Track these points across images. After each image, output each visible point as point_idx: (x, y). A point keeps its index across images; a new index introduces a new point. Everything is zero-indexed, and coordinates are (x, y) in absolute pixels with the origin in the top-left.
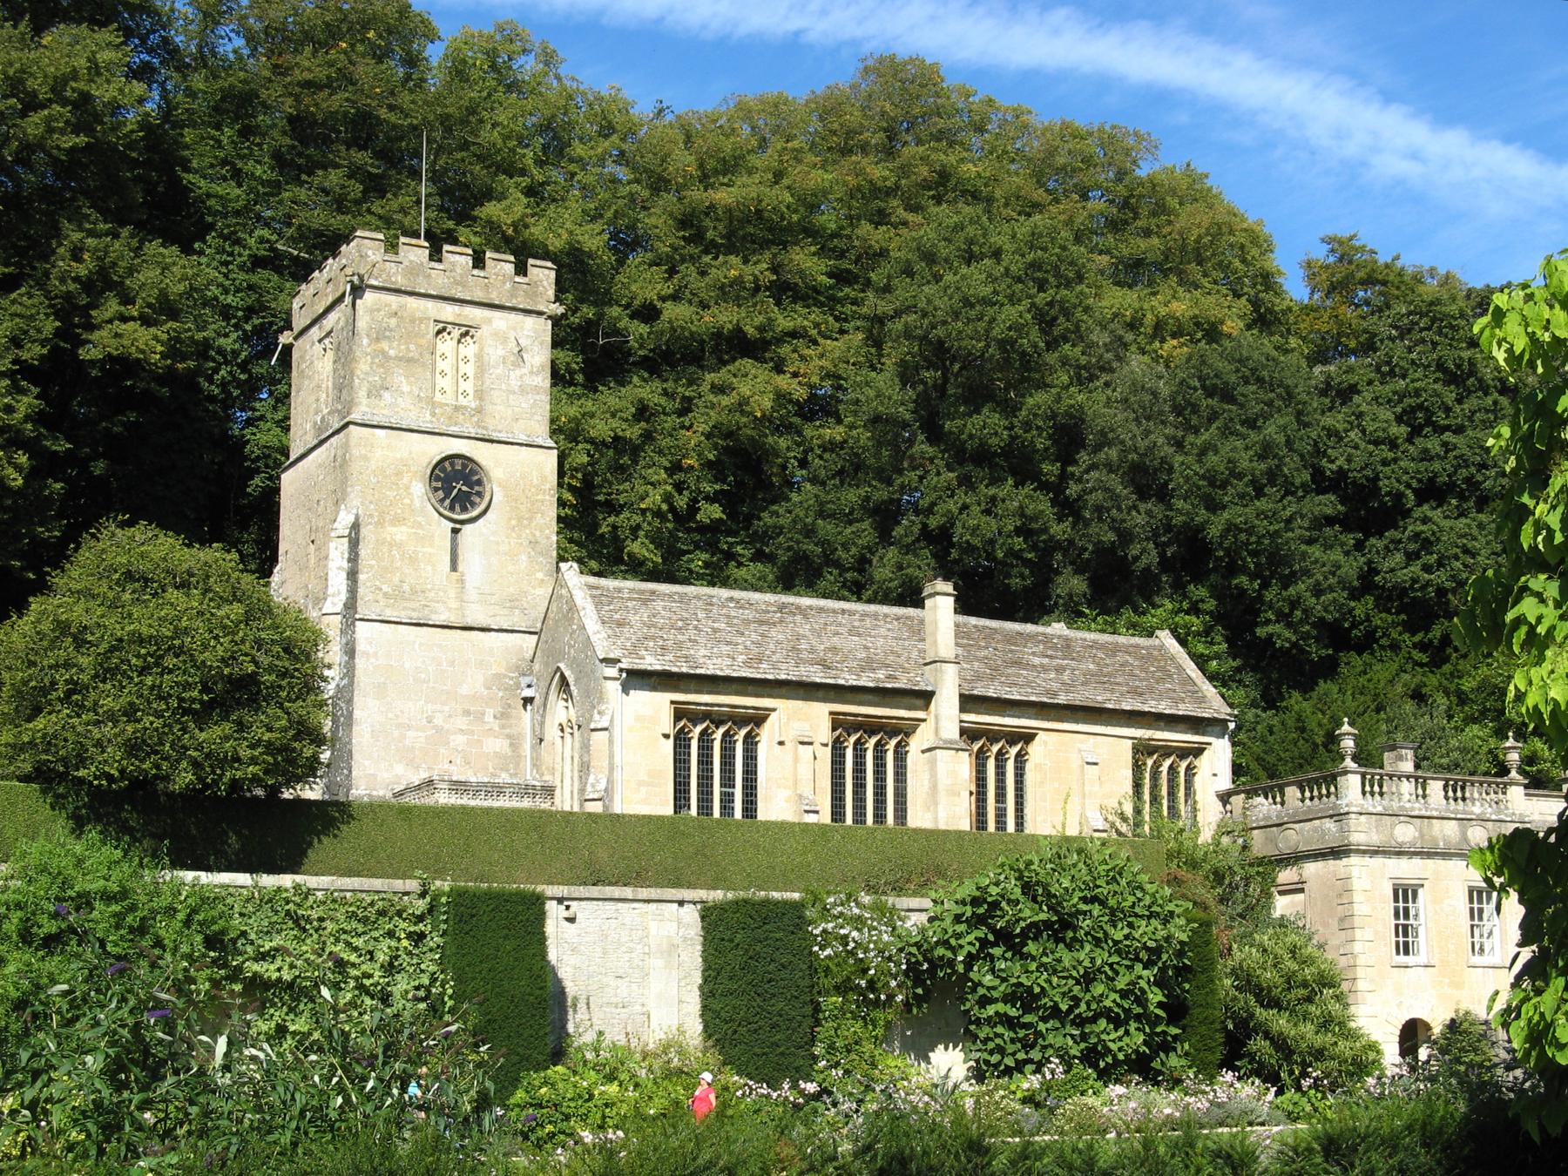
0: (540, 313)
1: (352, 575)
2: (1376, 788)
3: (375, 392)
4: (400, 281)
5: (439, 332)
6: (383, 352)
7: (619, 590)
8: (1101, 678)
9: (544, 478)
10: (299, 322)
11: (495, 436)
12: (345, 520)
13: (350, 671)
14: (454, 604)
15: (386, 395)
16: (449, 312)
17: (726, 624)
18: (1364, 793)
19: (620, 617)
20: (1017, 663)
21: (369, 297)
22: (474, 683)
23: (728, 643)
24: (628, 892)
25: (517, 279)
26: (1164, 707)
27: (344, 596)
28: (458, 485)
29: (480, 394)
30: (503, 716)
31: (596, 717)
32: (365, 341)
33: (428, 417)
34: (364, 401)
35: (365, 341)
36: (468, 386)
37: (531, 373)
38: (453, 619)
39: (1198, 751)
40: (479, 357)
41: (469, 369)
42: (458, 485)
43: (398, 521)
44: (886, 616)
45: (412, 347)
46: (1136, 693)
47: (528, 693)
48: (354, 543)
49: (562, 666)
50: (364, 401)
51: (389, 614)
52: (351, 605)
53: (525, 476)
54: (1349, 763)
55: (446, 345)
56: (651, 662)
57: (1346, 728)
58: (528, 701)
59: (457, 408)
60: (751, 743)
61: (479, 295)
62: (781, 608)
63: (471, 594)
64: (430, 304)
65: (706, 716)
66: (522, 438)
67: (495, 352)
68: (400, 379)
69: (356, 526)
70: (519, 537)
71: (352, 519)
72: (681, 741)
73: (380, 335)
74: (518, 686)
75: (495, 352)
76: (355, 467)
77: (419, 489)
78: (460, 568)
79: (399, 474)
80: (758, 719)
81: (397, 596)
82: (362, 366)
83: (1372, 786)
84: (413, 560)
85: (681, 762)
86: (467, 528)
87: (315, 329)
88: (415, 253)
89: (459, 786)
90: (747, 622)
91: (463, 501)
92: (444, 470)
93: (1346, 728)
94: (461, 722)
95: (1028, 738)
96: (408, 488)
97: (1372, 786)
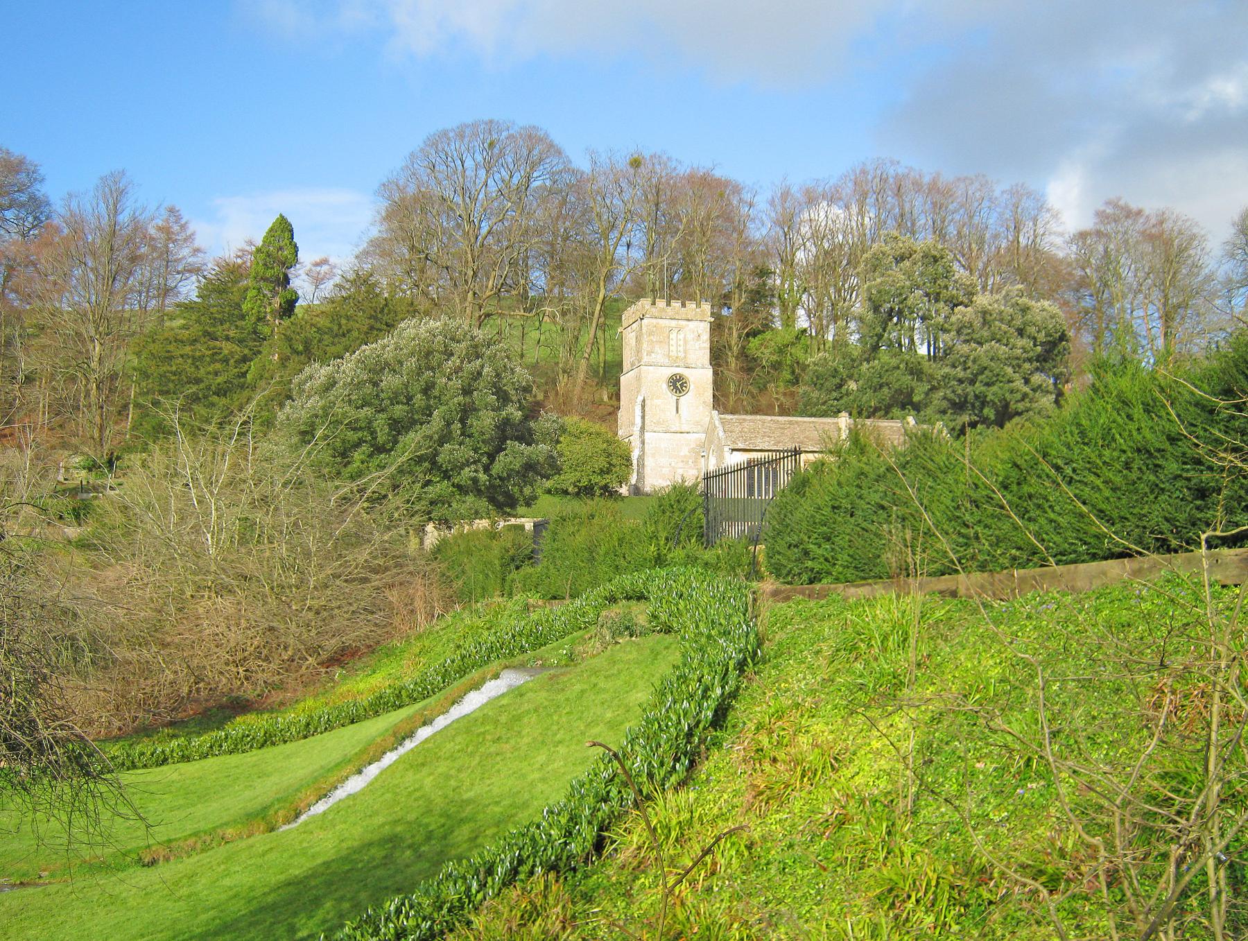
1: (643, 417)
10: (625, 324)
12: (640, 399)
13: (643, 450)
16: (674, 323)
22: (685, 451)
27: (640, 425)
28: (678, 384)
29: (685, 352)
30: (695, 462)
36: (681, 349)
41: (681, 343)
42: (678, 384)
48: (643, 407)
53: (701, 377)
56: (741, 446)
62: (790, 423)
63: (683, 421)
67: (690, 336)
73: (651, 334)
75: (690, 336)
77: (665, 386)
81: (658, 423)
82: (645, 345)
88: (661, 303)
94: (681, 465)
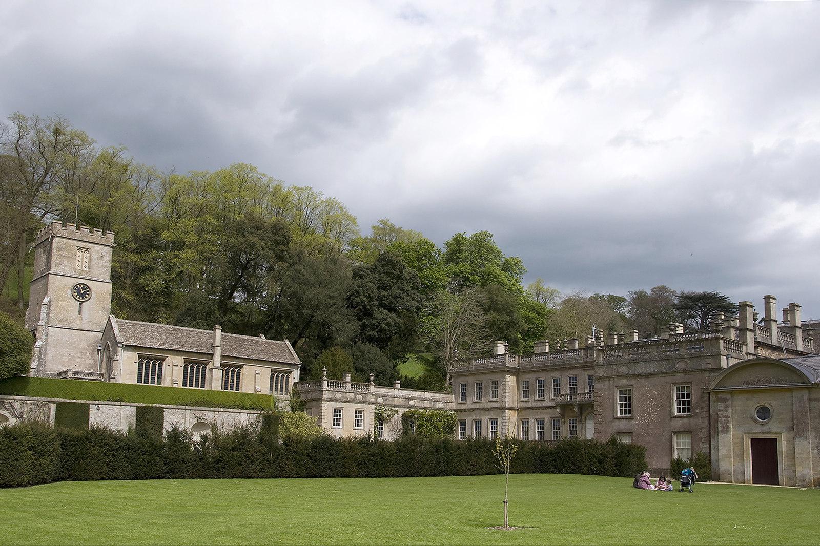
0: (109, 246)
1: (48, 315)
2: (332, 384)
3: (58, 265)
4: (67, 235)
5: (78, 250)
6: (60, 254)
7: (127, 323)
8: (265, 352)
9: (109, 289)
11: (94, 279)
14: (78, 323)
15: (61, 266)
16: (81, 244)
17: (155, 334)
18: (328, 385)
19: (123, 330)
20: (241, 347)
21: (56, 239)
22: (84, 344)
23: (156, 338)
24: (116, 403)
25: (103, 236)
26: (281, 360)
28: (82, 293)
29: (89, 267)
31: (116, 357)
32: (55, 251)
33: (74, 273)
34: (54, 268)
35: (55, 251)
36: (86, 265)
37: (106, 262)
38: (79, 328)
39: (290, 372)
40: (90, 257)
41: (87, 260)
43: (63, 300)
44: (205, 333)
45: (69, 253)
46: (274, 356)
47: (100, 348)
49: (108, 342)
50: (54, 268)
51: (58, 325)
52: (47, 323)
53: (103, 290)
54: (325, 378)
55: (79, 253)
56: (132, 343)
57: (325, 369)
58: (99, 350)
59: (82, 271)
60: (161, 365)
61: (91, 240)
64: (76, 242)
65: (148, 358)
66: (102, 280)
68: (65, 262)
69: (50, 302)
70: (99, 306)
71: (49, 299)
72: (140, 364)
73: (60, 249)
74: (97, 346)
75: (95, 256)
76: (50, 285)
78: (82, 314)
79: (64, 288)
80: (163, 359)
81: (62, 320)
82: (54, 258)
83: (331, 384)
84: (67, 312)
85: (140, 369)
86: (84, 304)
87: (42, 244)
88: (72, 228)
89: (74, 373)
90: (163, 333)
91: (83, 295)
92: (77, 287)
93: (325, 369)
95: (241, 367)
96: (66, 292)
97: (331, 384)
